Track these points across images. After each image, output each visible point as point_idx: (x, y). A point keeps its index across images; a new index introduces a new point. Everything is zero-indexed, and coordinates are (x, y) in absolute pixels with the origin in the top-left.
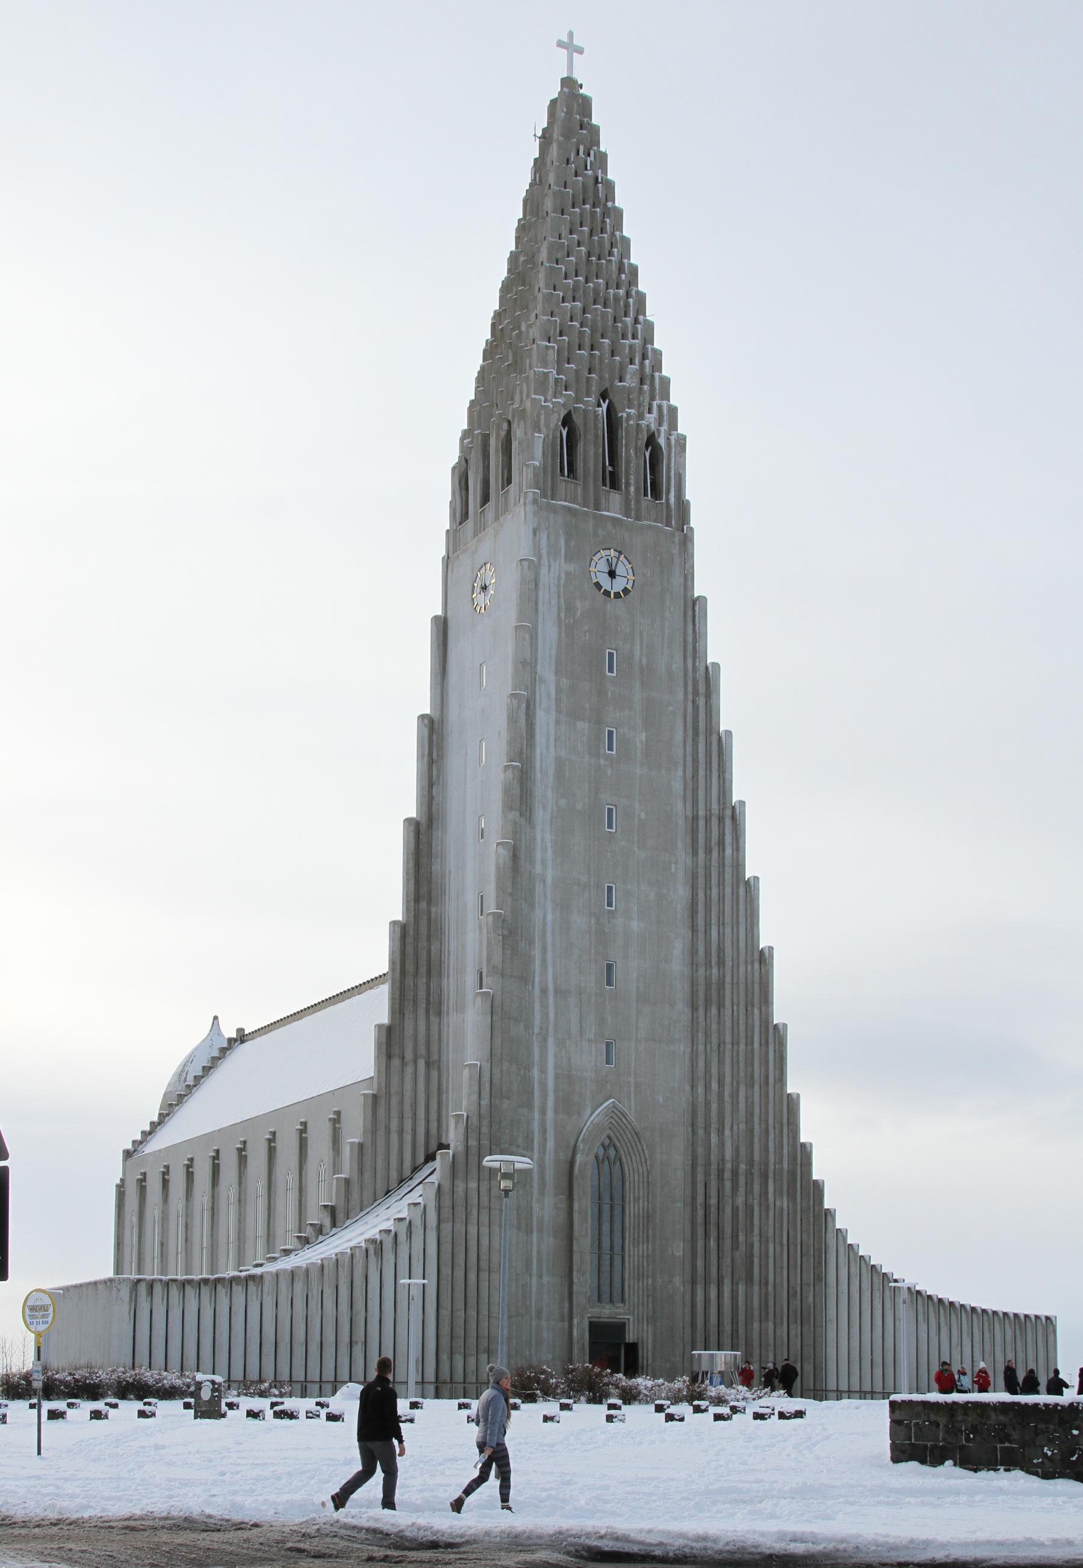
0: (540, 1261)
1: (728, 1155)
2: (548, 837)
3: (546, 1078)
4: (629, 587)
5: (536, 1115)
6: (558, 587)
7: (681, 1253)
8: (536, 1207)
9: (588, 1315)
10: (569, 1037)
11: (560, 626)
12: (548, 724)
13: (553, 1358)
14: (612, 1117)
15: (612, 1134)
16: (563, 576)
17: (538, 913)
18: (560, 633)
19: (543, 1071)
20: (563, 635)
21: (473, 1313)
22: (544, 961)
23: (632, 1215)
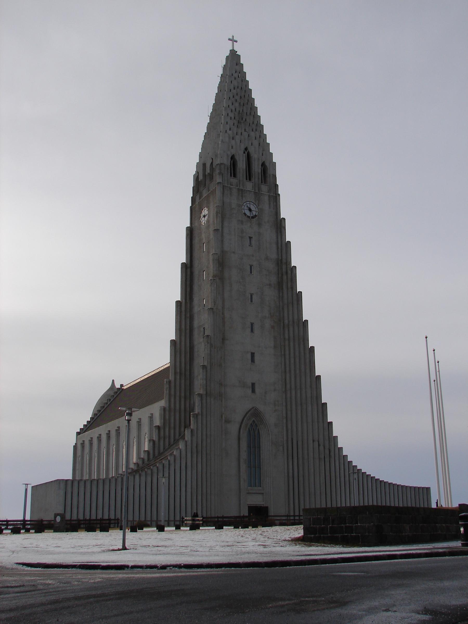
4: (257, 214)
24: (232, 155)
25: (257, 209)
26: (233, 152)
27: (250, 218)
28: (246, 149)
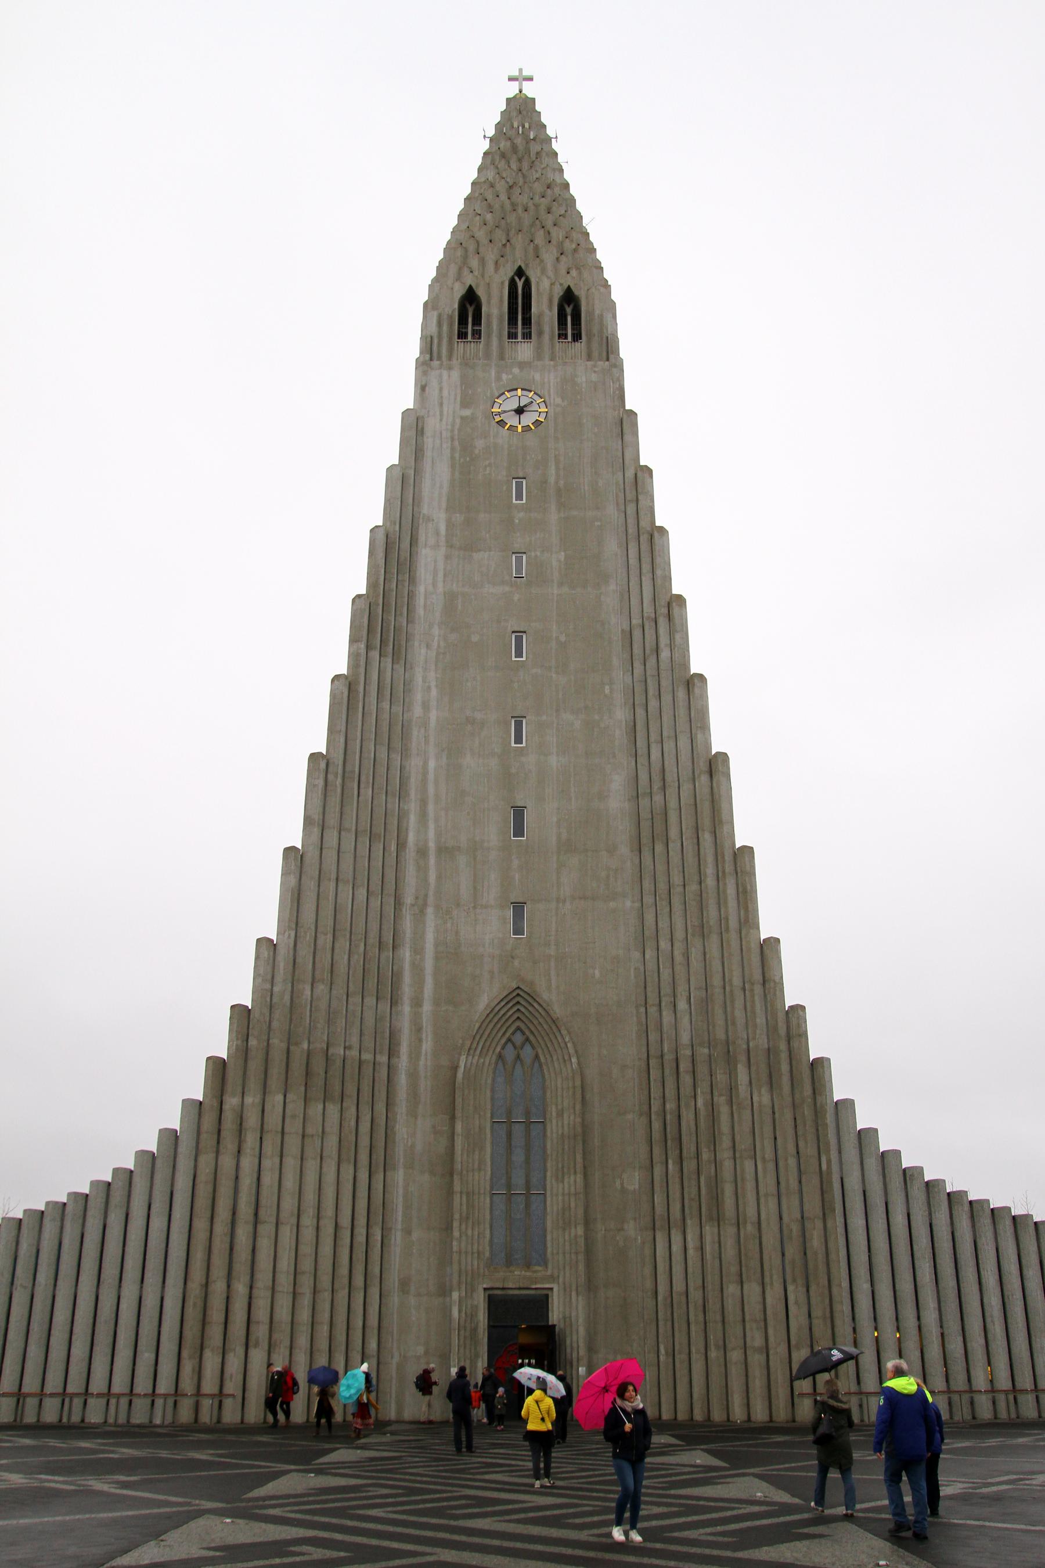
0: (407, 1207)
1: (685, 1038)
2: (432, 675)
3: (422, 959)
5: (406, 1009)
6: (452, 431)
7: (637, 1187)
8: (401, 1130)
9: (485, 1286)
10: (458, 905)
11: (453, 467)
12: (435, 561)
13: (426, 1353)
14: (518, 1003)
15: (523, 1027)
16: (458, 421)
17: (414, 763)
18: (453, 474)
19: (418, 950)
20: (457, 474)
21: (240, 1288)
22: (423, 815)
23: (555, 1135)
24: (467, 287)
25: (543, 405)
26: (469, 280)
27: (520, 430)
28: (520, 272)
